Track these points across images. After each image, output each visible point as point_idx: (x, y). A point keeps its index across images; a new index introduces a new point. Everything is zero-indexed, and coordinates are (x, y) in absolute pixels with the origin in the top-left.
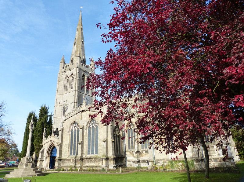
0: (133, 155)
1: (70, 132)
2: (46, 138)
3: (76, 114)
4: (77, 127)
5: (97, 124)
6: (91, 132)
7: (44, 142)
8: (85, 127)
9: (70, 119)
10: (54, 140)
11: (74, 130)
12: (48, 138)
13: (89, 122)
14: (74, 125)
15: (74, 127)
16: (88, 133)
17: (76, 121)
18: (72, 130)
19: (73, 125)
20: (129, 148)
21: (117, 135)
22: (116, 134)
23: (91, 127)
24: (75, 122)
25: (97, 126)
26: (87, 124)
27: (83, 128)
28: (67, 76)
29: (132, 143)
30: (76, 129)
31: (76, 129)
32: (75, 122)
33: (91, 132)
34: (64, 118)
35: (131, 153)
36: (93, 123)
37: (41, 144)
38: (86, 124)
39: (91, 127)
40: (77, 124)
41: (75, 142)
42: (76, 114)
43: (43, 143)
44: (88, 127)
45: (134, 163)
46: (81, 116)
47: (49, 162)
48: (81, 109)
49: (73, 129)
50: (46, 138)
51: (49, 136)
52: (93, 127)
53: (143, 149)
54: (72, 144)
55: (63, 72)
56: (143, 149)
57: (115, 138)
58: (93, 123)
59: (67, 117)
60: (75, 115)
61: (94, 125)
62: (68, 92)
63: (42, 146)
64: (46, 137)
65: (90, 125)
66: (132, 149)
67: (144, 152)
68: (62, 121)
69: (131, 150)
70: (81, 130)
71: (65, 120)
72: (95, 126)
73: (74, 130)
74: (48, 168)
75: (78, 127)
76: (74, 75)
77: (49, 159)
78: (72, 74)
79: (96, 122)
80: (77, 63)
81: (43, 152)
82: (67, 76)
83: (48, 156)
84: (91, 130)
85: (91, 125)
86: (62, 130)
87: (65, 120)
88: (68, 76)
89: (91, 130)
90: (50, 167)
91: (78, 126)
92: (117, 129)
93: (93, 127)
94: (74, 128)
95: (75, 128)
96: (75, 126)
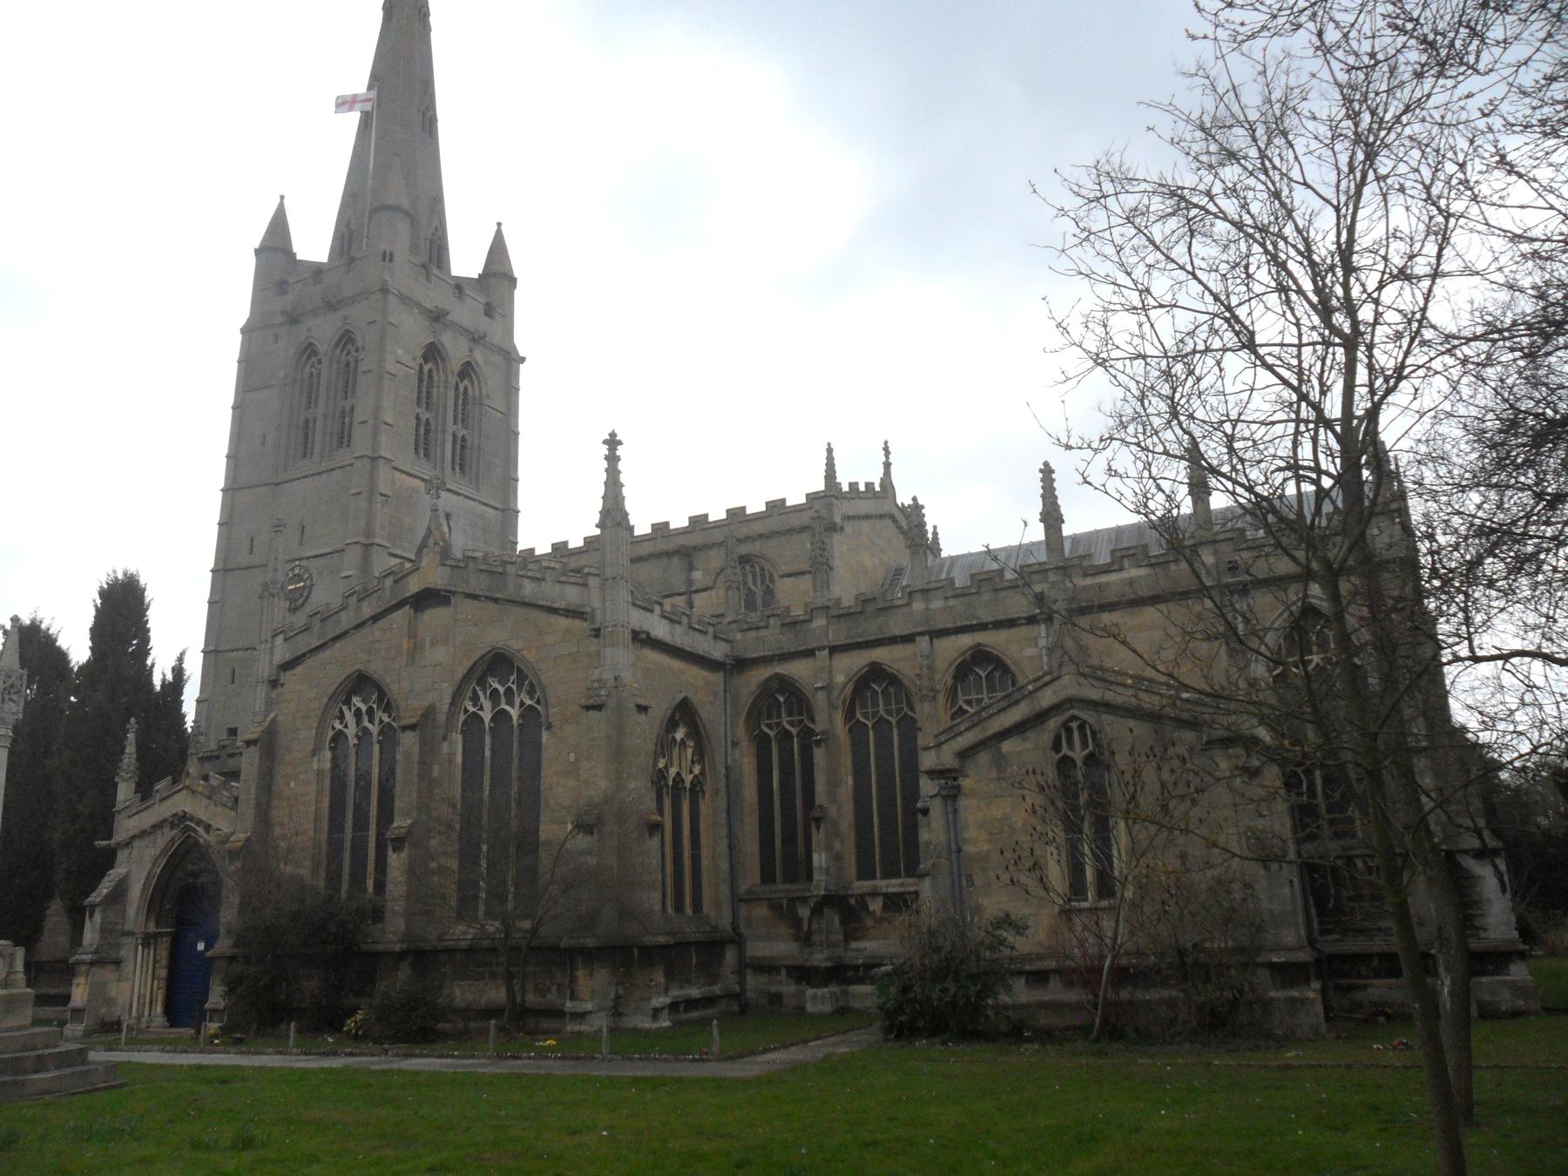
0: (796, 922)
1: (328, 754)
2: (143, 799)
3: (375, 618)
4: (381, 715)
5: (531, 693)
6: (488, 753)
7: (126, 827)
8: (442, 718)
10: (201, 814)
11: (353, 741)
12: (158, 797)
14: (356, 701)
15: (358, 714)
16: (459, 759)
17: (375, 669)
18: (339, 737)
19: (348, 702)
20: (767, 876)
21: (679, 779)
22: (673, 771)
23: (487, 716)
24: (361, 683)
25: (528, 713)
26: (457, 696)
27: (425, 722)
28: (309, 351)
29: (789, 839)
30: (374, 729)
31: (374, 729)
32: (361, 683)
33: (488, 753)
34: (282, 653)
35: (775, 906)
36: (501, 690)
38: (447, 700)
39: (487, 716)
40: (382, 695)
41: (361, 823)
42: (375, 618)
43: (120, 836)
44: (462, 717)
45: (799, 981)
46: (412, 634)
47: (163, 973)
48: (414, 586)
49: (351, 731)
50: (143, 799)
52: (500, 716)
54: (342, 841)
55: (280, 319)
57: (667, 802)
58: (501, 690)
59: (304, 643)
60: (366, 630)
62: (325, 465)
63: (108, 859)
64: (144, 790)
65: (475, 699)
66: (786, 880)
67: (876, 906)
68: (264, 669)
69: (781, 889)
70: (409, 740)
72: (514, 713)
75: (386, 719)
76: (360, 344)
77: (164, 953)
78: (346, 339)
79: (522, 677)
80: (388, 257)
82: (309, 351)
83: (152, 928)
84: (488, 740)
85: (487, 704)
86: (268, 743)
88: (314, 353)
89: (488, 740)
91: (388, 709)
92: (680, 735)
93: (500, 716)
94: (358, 723)
96: (364, 708)
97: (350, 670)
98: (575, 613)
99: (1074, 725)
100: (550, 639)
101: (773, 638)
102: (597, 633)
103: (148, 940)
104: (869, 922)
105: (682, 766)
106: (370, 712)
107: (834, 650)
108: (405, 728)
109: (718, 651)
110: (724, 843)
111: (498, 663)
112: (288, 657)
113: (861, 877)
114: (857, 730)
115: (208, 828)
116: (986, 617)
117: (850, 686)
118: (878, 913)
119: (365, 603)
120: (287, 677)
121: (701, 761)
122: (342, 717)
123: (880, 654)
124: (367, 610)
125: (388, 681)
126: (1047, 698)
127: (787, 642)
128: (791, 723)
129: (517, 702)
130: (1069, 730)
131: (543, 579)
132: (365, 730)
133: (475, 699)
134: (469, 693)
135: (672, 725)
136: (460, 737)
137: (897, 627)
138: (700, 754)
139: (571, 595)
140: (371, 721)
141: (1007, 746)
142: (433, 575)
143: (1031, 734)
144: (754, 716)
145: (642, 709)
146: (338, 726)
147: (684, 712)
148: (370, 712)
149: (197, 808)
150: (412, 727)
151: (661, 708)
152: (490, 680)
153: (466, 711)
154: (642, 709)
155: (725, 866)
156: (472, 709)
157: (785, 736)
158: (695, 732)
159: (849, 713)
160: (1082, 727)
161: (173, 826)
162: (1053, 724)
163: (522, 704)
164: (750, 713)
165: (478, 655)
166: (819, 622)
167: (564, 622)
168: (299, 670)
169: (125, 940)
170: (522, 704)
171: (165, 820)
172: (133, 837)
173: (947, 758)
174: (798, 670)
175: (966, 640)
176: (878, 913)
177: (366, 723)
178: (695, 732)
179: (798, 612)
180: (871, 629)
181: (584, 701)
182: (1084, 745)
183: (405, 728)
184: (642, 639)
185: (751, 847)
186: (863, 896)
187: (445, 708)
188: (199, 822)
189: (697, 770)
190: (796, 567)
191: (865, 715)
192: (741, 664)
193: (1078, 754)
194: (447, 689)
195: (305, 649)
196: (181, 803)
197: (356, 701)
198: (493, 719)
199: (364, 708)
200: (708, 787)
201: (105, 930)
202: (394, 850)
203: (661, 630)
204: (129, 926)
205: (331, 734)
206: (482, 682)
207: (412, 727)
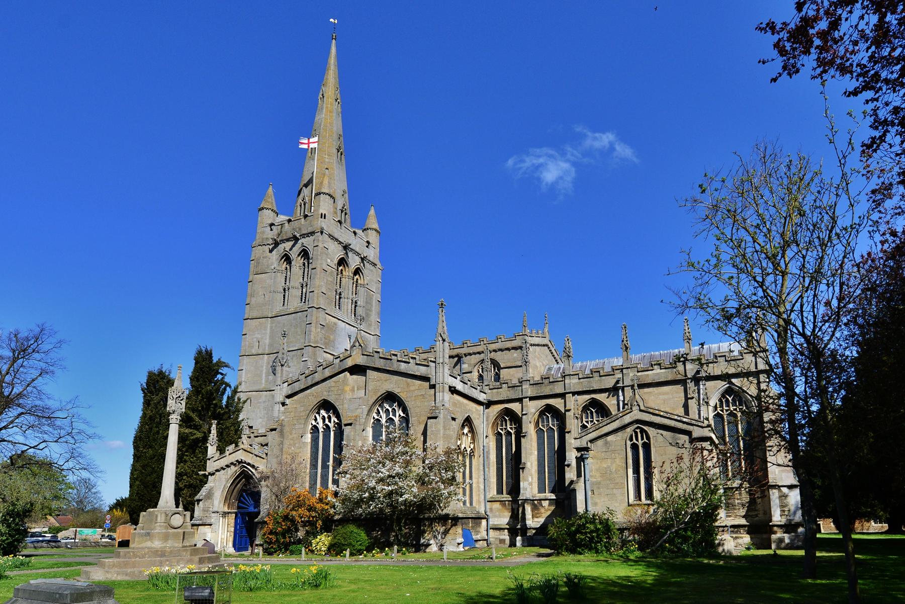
1: (309, 436)
4: (334, 419)
5: (405, 410)
9: (309, 391)
11: (321, 430)
12: (227, 453)
13: (374, 403)
17: (332, 399)
18: (315, 429)
19: (318, 413)
23: (383, 420)
24: (326, 405)
26: (370, 411)
31: (331, 425)
37: (201, 473)
39: (383, 420)
41: (325, 467)
48: (349, 363)
49: (320, 426)
51: (231, 448)
58: (390, 409)
61: (395, 415)
63: (204, 480)
65: (378, 413)
70: (347, 430)
72: (396, 419)
73: (321, 430)
74: (231, 550)
77: (232, 521)
81: (209, 496)
83: (226, 510)
85: (384, 416)
90: (234, 546)
92: (466, 430)
95: (327, 422)
96: (326, 416)
98: (425, 379)
99: (638, 430)
100: (412, 388)
101: (504, 393)
102: (433, 387)
103: (225, 514)
105: (466, 443)
106: (329, 418)
107: (531, 399)
108: (346, 425)
109: (482, 397)
110: (482, 477)
111: (390, 397)
114: (540, 432)
115: (253, 466)
116: (596, 387)
117: (538, 413)
121: (474, 443)
122: (316, 420)
123: (551, 401)
124: (327, 373)
125: (337, 405)
126: (627, 419)
127: (512, 395)
129: (397, 415)
130: (636, 433)
132: (327, 426)
133: (378, 413)
135: (463, 426)
137: (559, 389)
138: (473, 438)
139: (422, 371)
140: (330, 421)
141: (609, 438)
142: (360, 360)
143: (620, 434)
144: (495, 424)
145: (454, 419)
146: (314, 423)
147: (468, 421)
148: (329, 418)
149: (249, 458)
150: (350, 424)
151: (460, 420)
154: (454, 419)
155: (482, 487)
156: (376, 417)
157: (509, 434)
158: (472, 430)
161: (235, 465)
162: (629, 430)
164: (494, 423)
165: (380, 394)
166: (526, 386)
167: (418, 382)
168: (295, 398)
169: (213, 515)
171: (232, 464)
172: (217, 471)
173: (583, 443)
174: (515, 407)
175: (587, 397)
177: (327, 422)
178: (472, 430)
179: (515, 381)
180: (547, 390)
181: (429, 415)
182: (642, 439)
183: (346, 425)
184: (453, 390)
185: (493, 480)
188: (249, 464)
189: (472, 446)
190: (509, 365)
191: (543, 426)
192: (489, 404)
194: (365, 409)
196: (240, 455)
197: (323, 412)
199: (326, 416)
200: (476, 454)
201: (205, 510)
203: (460, 387)
204: (215, 509)
206: (381, 406)
207: (350, 424)
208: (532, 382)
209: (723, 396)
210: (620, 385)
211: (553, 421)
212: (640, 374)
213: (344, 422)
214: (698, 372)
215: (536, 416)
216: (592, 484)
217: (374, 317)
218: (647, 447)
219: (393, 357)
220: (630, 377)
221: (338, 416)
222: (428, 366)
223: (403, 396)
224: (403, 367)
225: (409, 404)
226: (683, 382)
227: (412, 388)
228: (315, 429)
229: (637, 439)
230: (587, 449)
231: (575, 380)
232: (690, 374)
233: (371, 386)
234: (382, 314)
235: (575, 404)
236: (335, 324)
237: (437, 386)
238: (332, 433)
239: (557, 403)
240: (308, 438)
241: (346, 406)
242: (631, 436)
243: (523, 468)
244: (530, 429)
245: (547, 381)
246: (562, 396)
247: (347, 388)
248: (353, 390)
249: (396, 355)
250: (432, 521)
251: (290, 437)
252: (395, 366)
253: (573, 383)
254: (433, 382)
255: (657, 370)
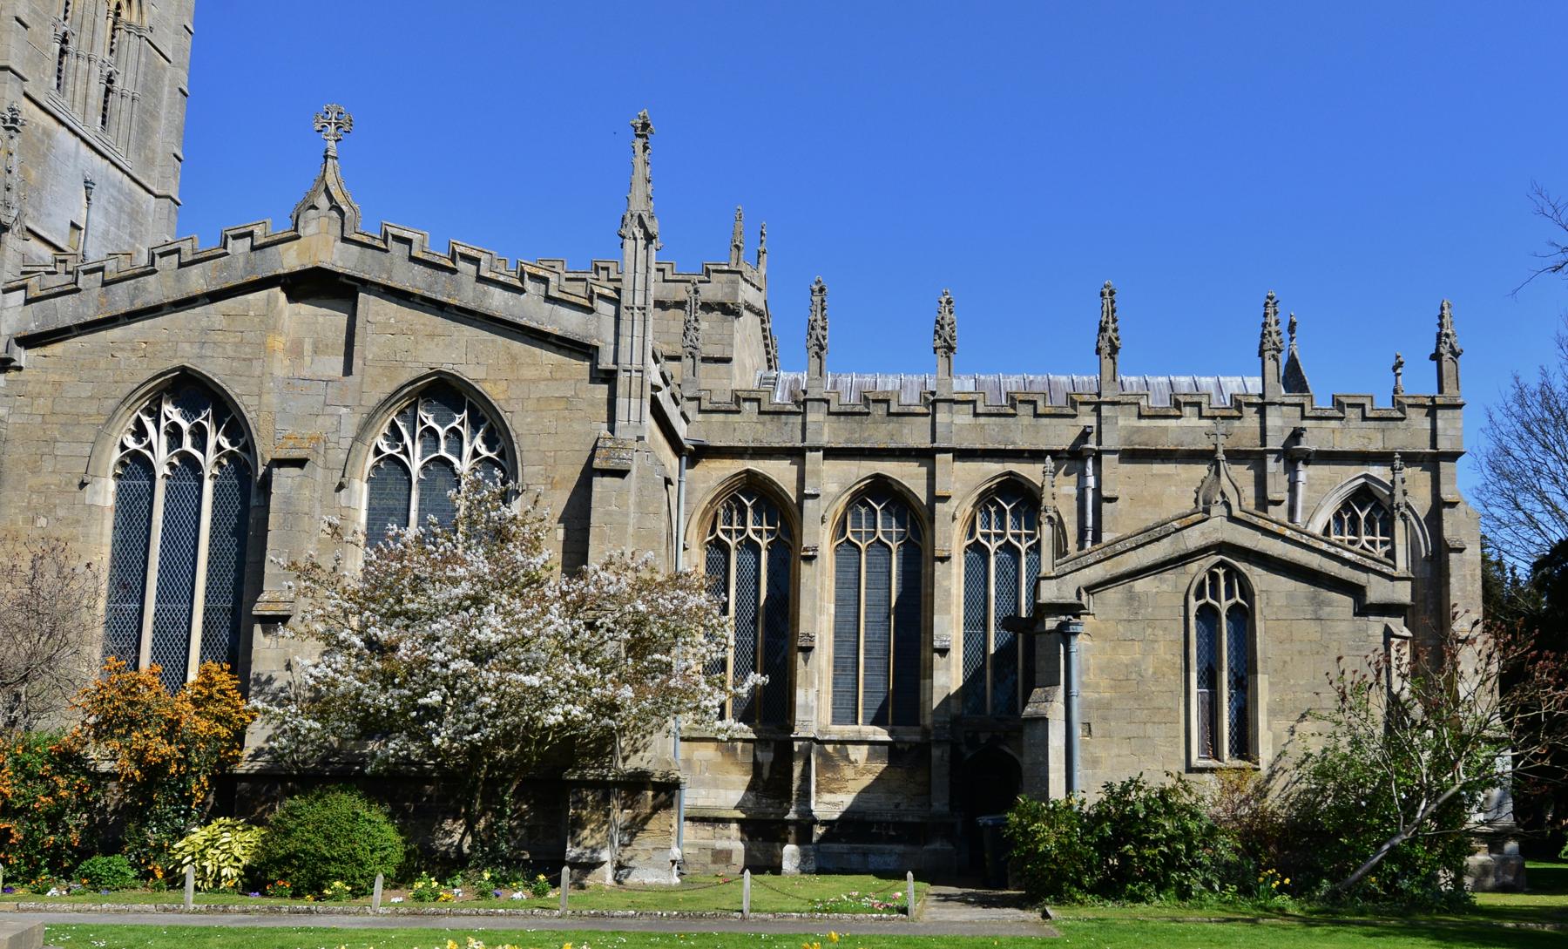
1: (112, 485)
13: (386, 404)
14: (167, 408)
15: (175, 434)
17: (214, 369)
24: (190, 388)
48: (290, 259)
49: (161, 458)
53: (848, 731)
56: (848, 731)
59: (66, 311)
71: (28, 342)
73: (161, 469)
85: (416, 450)
87: (28, 342)
95: (187, 444)
97: (176, 363)
99: (1221, 572)
104: (848, 772)
111: (445, 391)
112: (33, 327)
113: (836, 720)
114: (846, 549)
117: (846, 498)
118: (861, 764)
119: (195, 270)
120: (22, 356)
122: (140, 432)
124: (198, 280)
126: (1194, 538)
128: (727, 532)
129: (467, 450)
130: (1214, 577)
131: (521, 291)
134: (385, 429)
136: (365, 487)
137: (915, 435)
139: (567, 322)
141: (1140, 585)
143: (1169, 576)
150: (300, 463)
152: (421, 413)
153: (378, 452)
157: (751, 546)
159: (841, 527)
160: (1228, 577)
162: (1198, 569)
163: (476, 454)
166: (815, 416)
167: (549, 357)
168: (57, 349)
170: (476, 454)
175: (995, 468)
176: (861, 764)
177: (187, 444)
180: (879, 434)
182: (1230, 595)
186: (843, 742)
187: (346, 443)
193: (1224, 606)
195: (68, 321)
197: (167, 408)
198: (424, 468)
202: (265, 631)
205: (117, 455)
208: (834, 408)
209: (1346, 506)
210: (1092, 445)
211: (887, 524)
212: (1145, 423)
213: (266, 450)
214: (1297, 435)
215: (840, 505)
216: (1088, 706)
217: (166, 139)
218: (1243, 617)
219: (462, 265)
220: (1120, 428)
221: (236, 427)
222: (590, 311)
223: (494, 391)
224: (497, 302)
225: (518, 423)
226: (1254, 459)
227: (528, 373)
228: (137, 465)
229: (1215, 595)
230: (1075, 610)
231: (963, 417)
232: (1275, 442)
233: (369, 346)
234: (191, 132)
235: (962, 483)
236: (47, 133)
237: (622, 377)
238: (208, 486)
239: (909, 475)
240: (106, 492)
241: (272, 400)
242: (1202, 583)
243: (808, 650)
244: (819, 535)
245: (880, 410)
246: (926, 456)
247: (279, 343)
248: (296, 351)
249: (475, 261)
250: (605, 789)
251: (32, 481)
252: (466, 293)
253: (957, 426)
254: (606, 362)
255: (1190, 420)
